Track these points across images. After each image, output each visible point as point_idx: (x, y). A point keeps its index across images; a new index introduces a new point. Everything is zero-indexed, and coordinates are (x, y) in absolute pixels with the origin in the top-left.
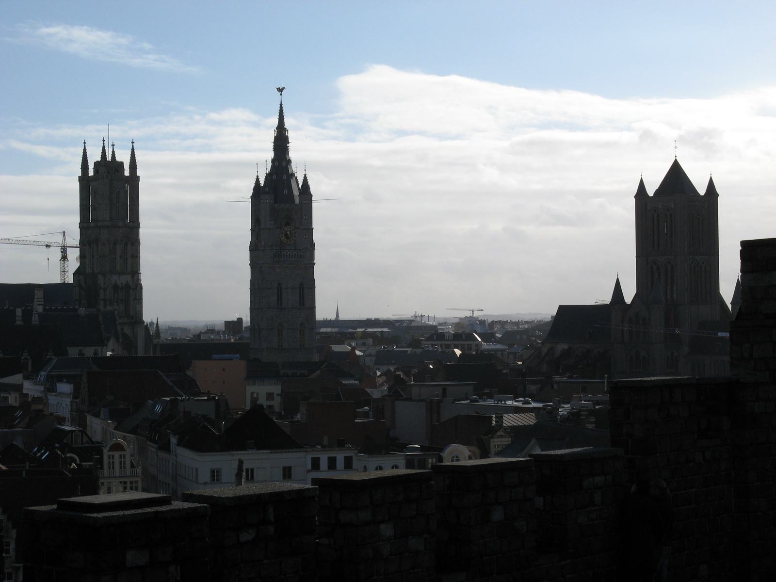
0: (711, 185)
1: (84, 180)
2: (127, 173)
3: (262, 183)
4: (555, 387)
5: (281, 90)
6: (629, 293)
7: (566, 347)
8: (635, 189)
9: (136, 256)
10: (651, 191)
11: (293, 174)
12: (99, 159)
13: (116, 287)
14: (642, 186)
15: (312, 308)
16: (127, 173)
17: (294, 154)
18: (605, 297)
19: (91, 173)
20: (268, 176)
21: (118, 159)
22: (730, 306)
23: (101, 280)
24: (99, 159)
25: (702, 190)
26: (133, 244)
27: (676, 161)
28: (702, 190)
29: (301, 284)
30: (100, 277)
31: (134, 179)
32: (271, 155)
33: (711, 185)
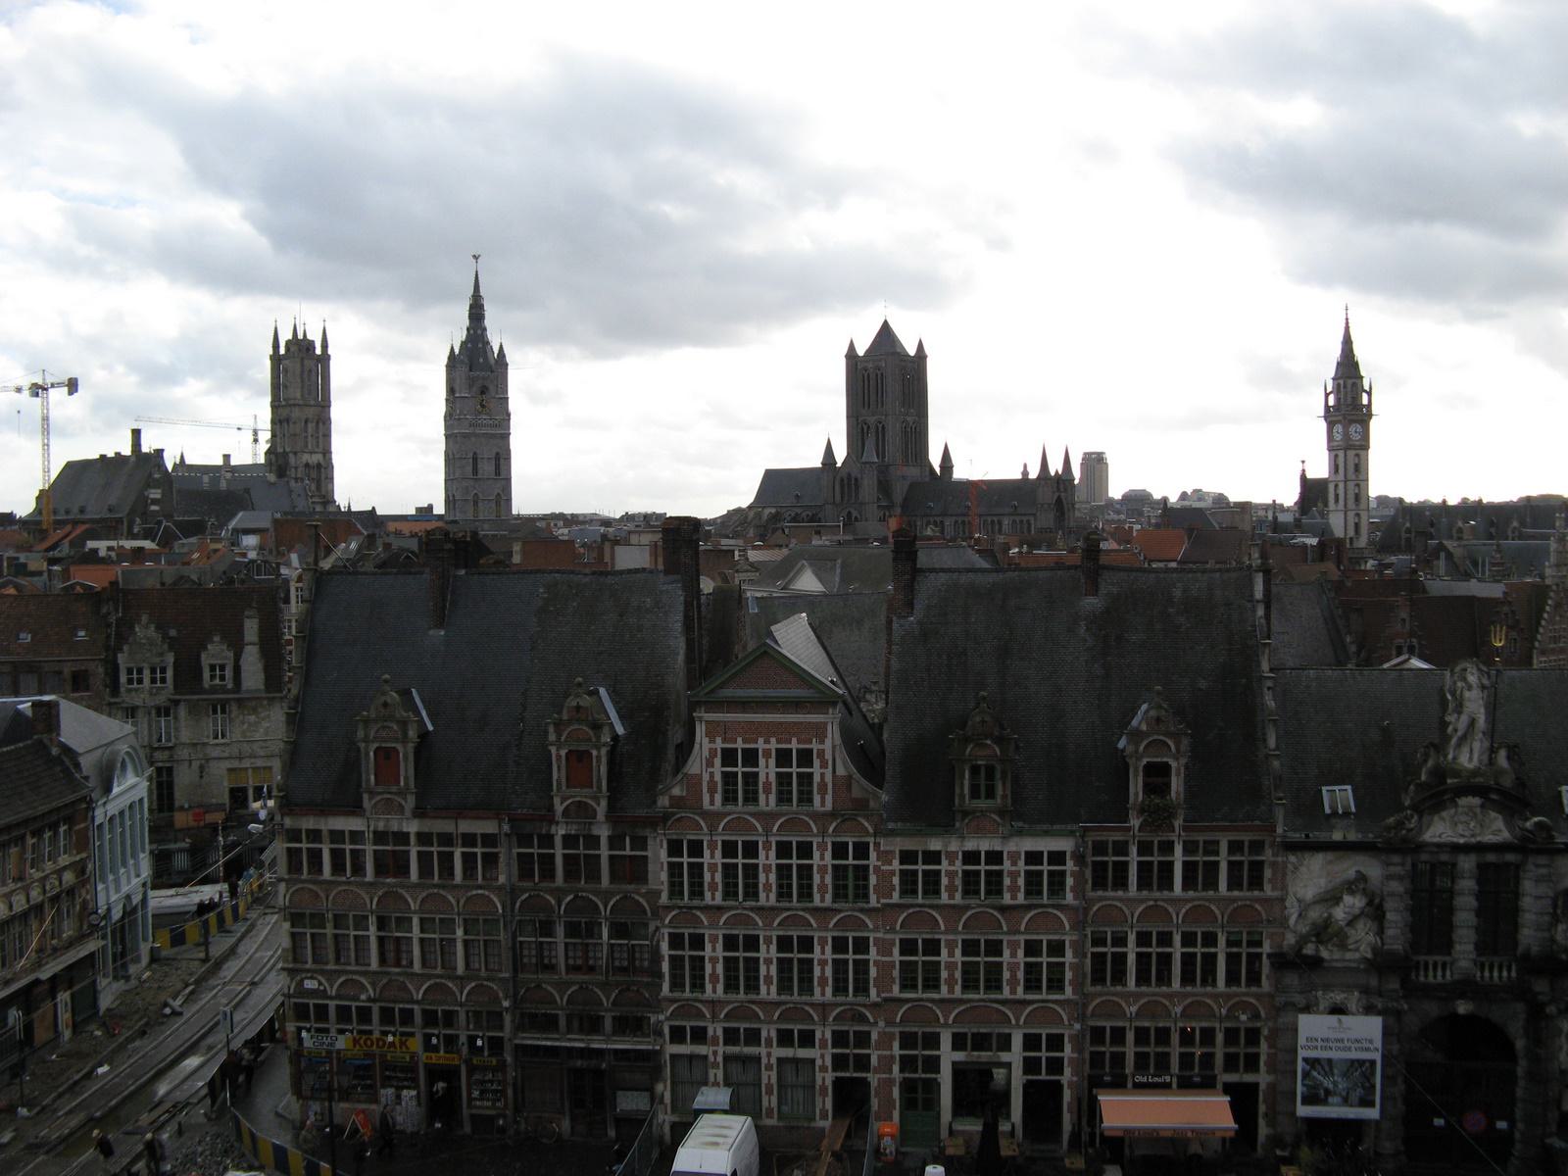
0: (920, 346)
1: (276, 358)
2: (318, 351)
3: (457, 351)
4: (787, 531)
5: (476, 257)
6: (840, 454)
7: (773, 511)
8: (845, 350)
9: (327, 436)
10: (861, 351)
11: (488, 343)
12: (290, 337)
13: (307, 465)
14: (852, 347)
15: (508, 480)
16: (318, 351)
17: (487, 322)
18: (815, 461)
19: (282, 351)
20: (463, 344)
21: (309, 337)
22: (938, 470)
23: (292, 459)
24: (290, 337)
25: (912, 351)
26: (324, 423)
27: (886, 322)
28: (912, 351)
29: (497, 454)
30: (291, 455)
31: (325, 358)
32: (467, 322)
33: (920, 346)
